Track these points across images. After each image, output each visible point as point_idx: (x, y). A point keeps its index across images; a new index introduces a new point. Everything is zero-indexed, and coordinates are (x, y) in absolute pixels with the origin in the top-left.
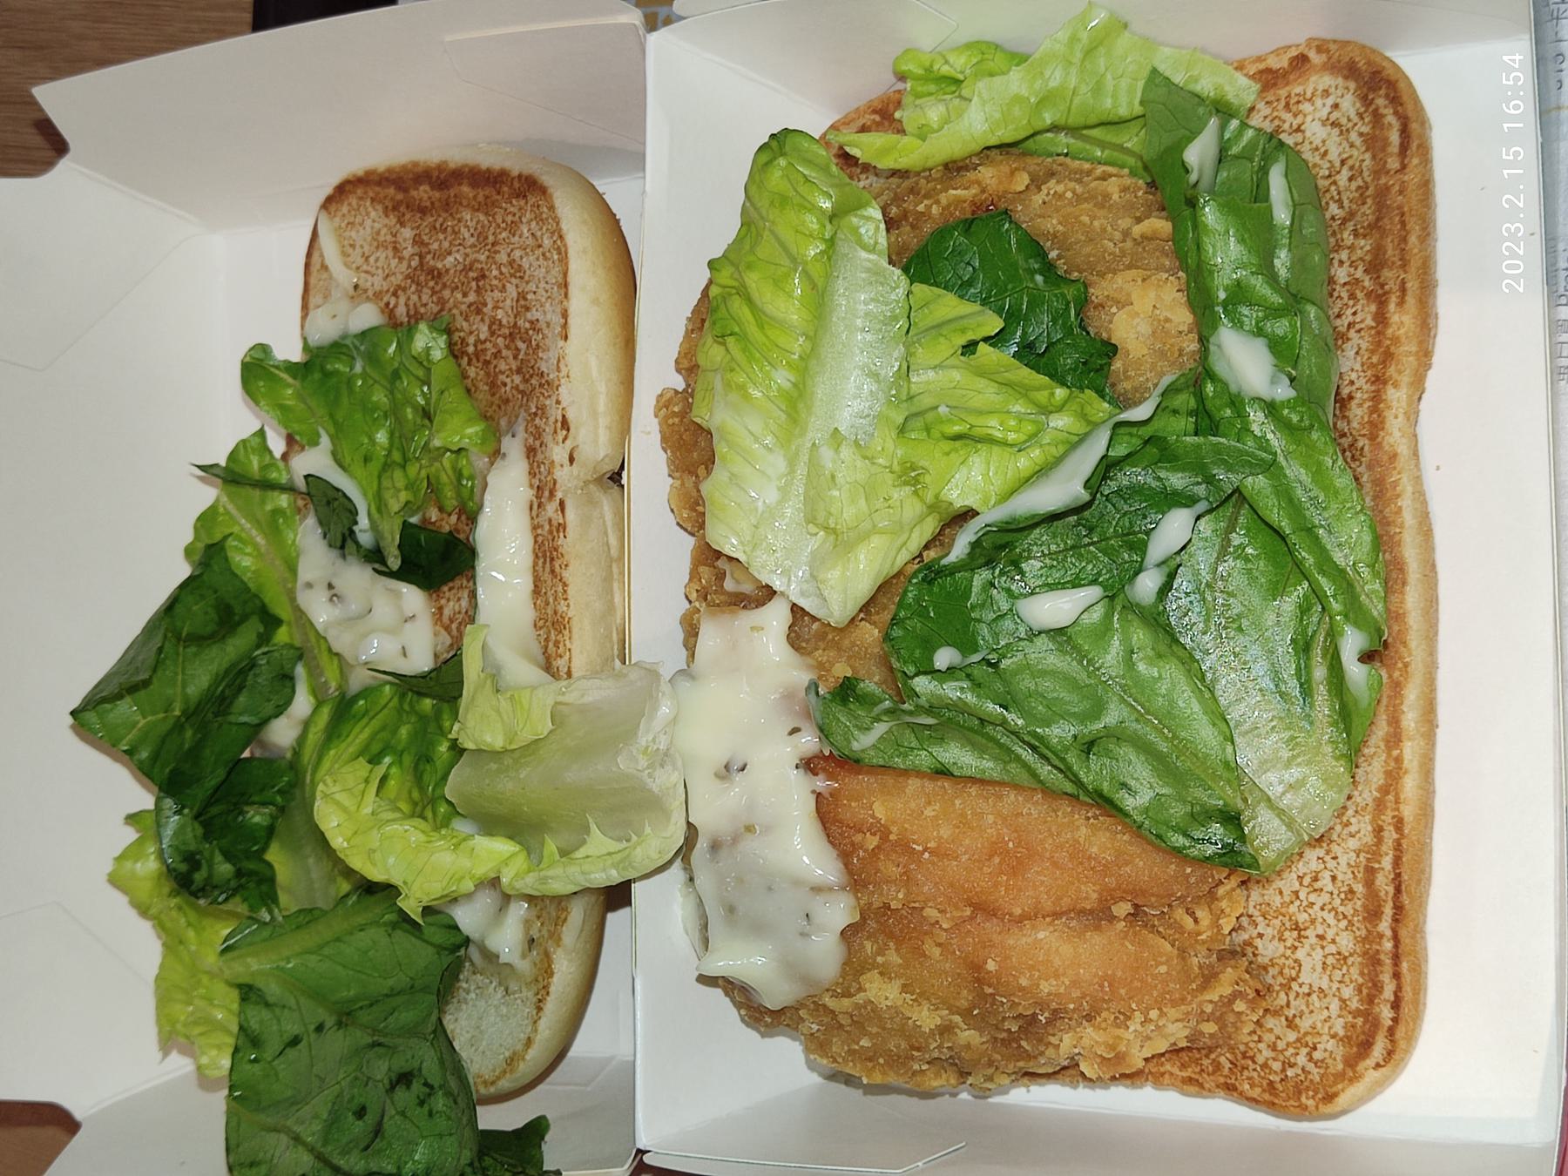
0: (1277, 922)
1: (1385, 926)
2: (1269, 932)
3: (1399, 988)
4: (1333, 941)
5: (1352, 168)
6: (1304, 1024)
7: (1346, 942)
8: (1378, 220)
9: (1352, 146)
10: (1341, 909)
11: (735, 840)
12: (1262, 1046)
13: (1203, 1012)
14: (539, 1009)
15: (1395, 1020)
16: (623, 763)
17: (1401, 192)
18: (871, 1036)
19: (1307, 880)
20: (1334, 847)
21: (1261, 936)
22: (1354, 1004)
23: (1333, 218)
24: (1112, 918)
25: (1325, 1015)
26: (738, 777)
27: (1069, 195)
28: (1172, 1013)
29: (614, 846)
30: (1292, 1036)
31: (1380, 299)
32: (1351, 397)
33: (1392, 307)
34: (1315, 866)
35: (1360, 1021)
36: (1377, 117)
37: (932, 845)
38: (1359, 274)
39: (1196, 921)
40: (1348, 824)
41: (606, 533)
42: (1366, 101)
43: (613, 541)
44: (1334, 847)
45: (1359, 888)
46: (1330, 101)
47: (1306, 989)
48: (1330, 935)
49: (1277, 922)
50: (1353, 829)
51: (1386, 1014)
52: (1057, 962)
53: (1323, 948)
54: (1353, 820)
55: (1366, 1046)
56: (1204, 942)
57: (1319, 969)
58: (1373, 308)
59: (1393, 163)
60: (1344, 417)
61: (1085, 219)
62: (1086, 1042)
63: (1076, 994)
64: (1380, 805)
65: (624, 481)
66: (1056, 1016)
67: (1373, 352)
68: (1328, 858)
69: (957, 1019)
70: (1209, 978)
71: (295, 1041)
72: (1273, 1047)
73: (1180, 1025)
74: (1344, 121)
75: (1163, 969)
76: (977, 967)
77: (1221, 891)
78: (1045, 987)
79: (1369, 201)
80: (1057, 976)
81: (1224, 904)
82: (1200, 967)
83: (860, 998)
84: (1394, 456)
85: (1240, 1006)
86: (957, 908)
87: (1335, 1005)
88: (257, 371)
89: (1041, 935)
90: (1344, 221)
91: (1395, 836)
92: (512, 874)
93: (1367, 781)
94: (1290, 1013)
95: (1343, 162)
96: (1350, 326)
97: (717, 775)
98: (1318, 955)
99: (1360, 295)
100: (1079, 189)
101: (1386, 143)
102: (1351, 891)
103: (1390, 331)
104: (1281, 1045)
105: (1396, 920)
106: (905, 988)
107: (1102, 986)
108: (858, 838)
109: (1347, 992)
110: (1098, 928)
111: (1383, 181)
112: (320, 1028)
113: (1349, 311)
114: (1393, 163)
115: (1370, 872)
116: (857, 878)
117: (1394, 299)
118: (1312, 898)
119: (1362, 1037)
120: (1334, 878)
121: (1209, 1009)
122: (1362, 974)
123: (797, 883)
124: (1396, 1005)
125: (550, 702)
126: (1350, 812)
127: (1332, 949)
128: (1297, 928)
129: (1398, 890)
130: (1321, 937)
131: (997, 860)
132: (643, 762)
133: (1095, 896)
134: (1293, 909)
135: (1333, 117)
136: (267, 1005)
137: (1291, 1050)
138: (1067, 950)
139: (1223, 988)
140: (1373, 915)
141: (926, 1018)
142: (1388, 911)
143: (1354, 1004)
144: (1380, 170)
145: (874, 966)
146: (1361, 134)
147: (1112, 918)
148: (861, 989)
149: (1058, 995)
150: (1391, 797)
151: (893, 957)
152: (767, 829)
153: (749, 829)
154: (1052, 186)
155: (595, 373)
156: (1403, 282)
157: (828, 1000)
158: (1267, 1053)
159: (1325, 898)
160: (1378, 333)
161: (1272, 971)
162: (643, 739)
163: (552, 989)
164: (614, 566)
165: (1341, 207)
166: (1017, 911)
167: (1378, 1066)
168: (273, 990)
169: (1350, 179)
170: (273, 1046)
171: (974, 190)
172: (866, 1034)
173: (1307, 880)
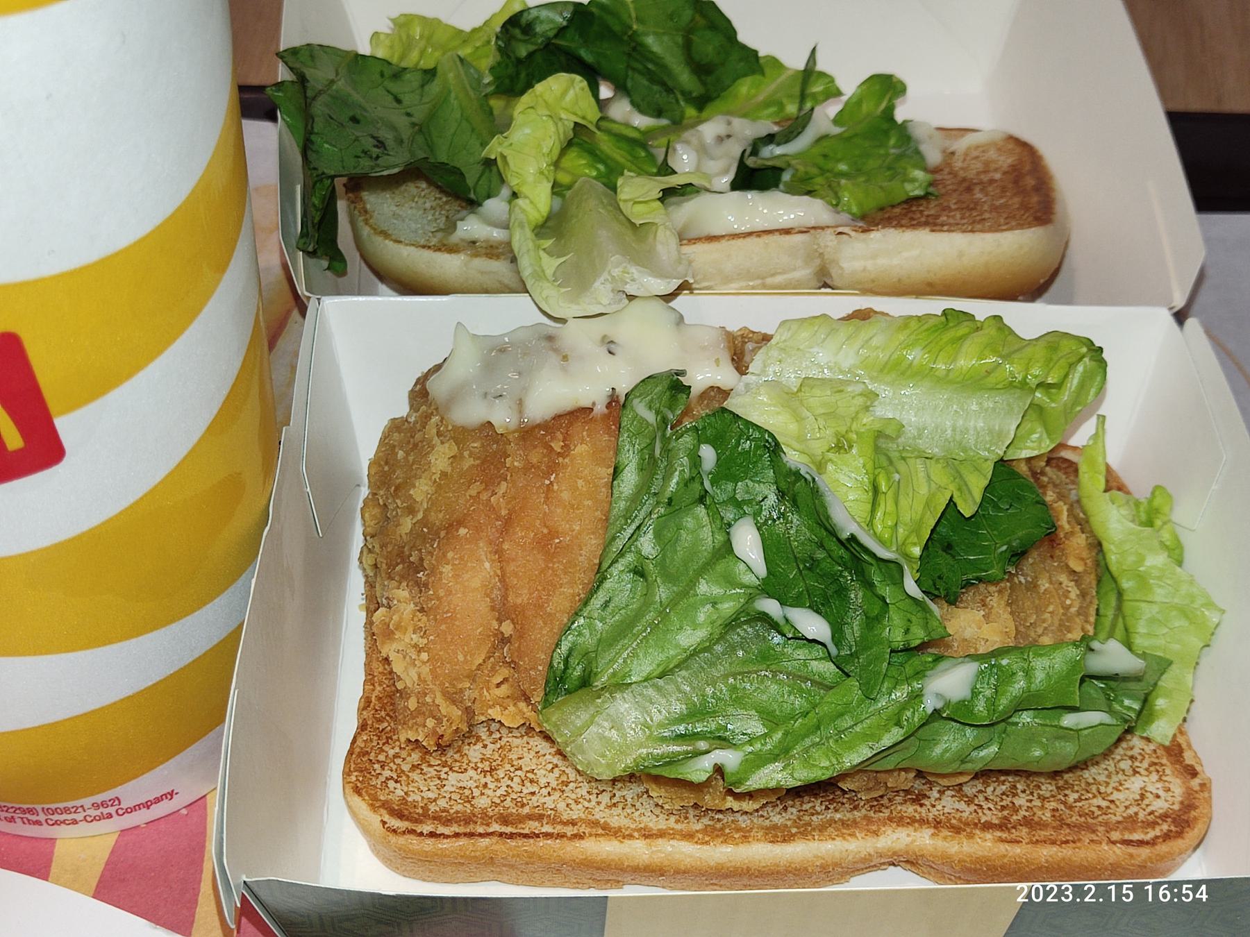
0: (496, 756)
1: (495, 827)
2: (488, 752)
3: (447, 837)
4: (482, 794)
5: (1108, 807)
6: (415, 776)
7: (482, 802)
8: (1068, 825)
9: (1127, 807)
10: (509, 799)
11: (556, 350)
12: (397, 750)
13: (426, 695)
14: (424, 247)
15: (421, 834)
16: (616, 258)
17: (1092, 841)
18: (406, 458)
20: (558, 794)
21: (485, 746)
22: (432, 808)
23: (1066, 795)
24: (500, 621)
25: (421, 789)
26: (604, 350)
27: (1068, 602)
28: (426, 670)
29: (549, 272)
30: (406, 767)
31: (1002, 826)
32: (921, 805)
33: (999, 834)
34: (543, 782)
35: (420, 811)
36: (1153, 824)
37: (556, 487)
38: (1023, 813)
39: (498, 685)
40: (577, 802)
41: (784, 272)
42: (1164, 817)
43: (778, 279)
44: (558, 794)
45: (526, 810)
46: (1161, 793)
47: (443, 776)
49: (496, 756)
50: (573, 806)
51: (426, 828)
52: (466, 576)
54: (580, 806)
55: (400, 815)
56: (481, 695)
57: (461, 784)
58: (996, 821)
59: (1115, 836)
60: (905, 801)
61: (1051, 608)
62: (402, 606)
63: (441, 593)
64: (596, 824)
65: (823, 290)
66: (422, 586)
67: (960, 820)
68: (549, 789)
69: (420, 516)
70: (453, 698)
71: (398, 101)
72: (396, 756)
73: (416, 678)
74: (1146, 802)
75: (461, 658)
76: (460, 523)
77: (522, 705)
78: (447, 569)
79: (1083, 819)
80: (456, 576)
81: (511, 708)
82: (462, 691)
83: (436, 440)
84: (876, 833)
85: (430, 723)
86: (507, 503)
87: (431, 795)
88: (887, 87)
89: (487, 565)
90: (1065, 803)
91: (569, 834)
92: (524, 206)
93: (611, 815)
94: (423, 766)
95: (1112, 801)
96: (980, 806)
97: (604, 337)
98: (472, 784)
99: (1005, 813)
100: (1073, 610)
101: (1133, 830)
102: (523, 805)
103: (977, 832)
104: (398, 761)
105: (501, 835)
106: (444, 474)
107: (447, 612)
108: (560, 436)
109: (442, 803)
110: (493, 609)
111: (1101, 829)
112: (408, 115)
113: (992, 807)
114: (1115, 836)
115: (540, 818)
116: (528, 433)
117: (1004, 835)
118: (517, 780)
119: (406, 813)
120: (533, 794)
121: (428, 699)
122: (457, 812)
123: (525, 389)
124: (432, 835)
125: (656, 221)
126: (586, 804)
127: (476, 793)
128: (492, 770)
129: (526, 836)
130: (485, 785)
131: (545, 531)
132: (616, 272)
133: (519, 601)
134: (508, 767)
135: (1148, 795)
136: (422, 86)
137: (394, 767)
138: (476, 583)
139: (445, 708)
140: (505, 820)
141: (421, 491)
142: (509, 830)
143: (432, 808)
144: (1109, 827)
145: (461, 450)
146: (1136, 814)
147: (500, 621)
148: (442, 443)
149: (440, 579)
150: (600, 831)
151: (468, 462)
152: (564, 370)
153: (565, 358)
154: (1074, 592)
155: (905, 254)
156: (1019, 842)
157: (435, 419)
158: (391, 752)
159: (517, 788)
160: (976, 825)
161: (457, 756)
162: (634, 270)
163: (438, 254)
164: (759, 282)
165: (1075, 801)
166: (506, 546)
167: (384, 823)
168: (435, 88)
169: (1099, 807)
170: (394, 87)
171: (1067, 527)
172: (408, 454)
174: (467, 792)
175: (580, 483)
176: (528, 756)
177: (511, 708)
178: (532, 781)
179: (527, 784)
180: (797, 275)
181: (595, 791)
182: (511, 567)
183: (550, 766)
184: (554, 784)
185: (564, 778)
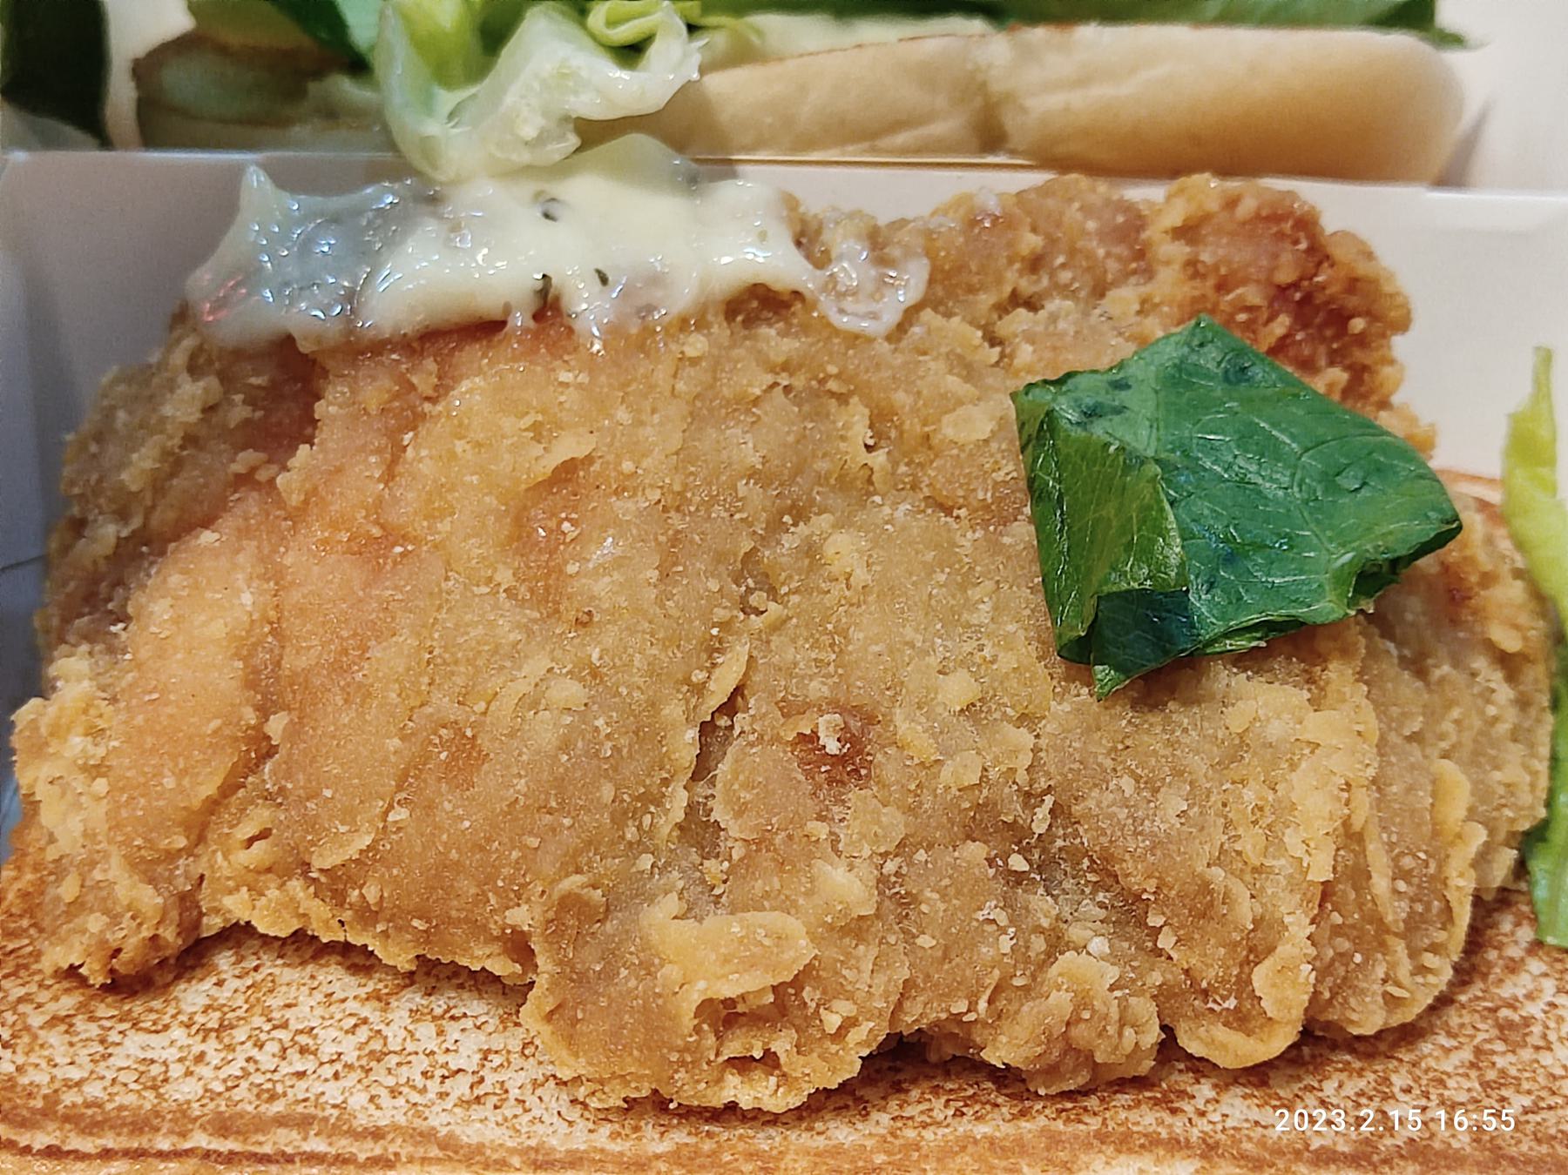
2: (223, 995)
4: (189, 1073)
19: (303, 1040)
20: (359, 1074)
21: (219, 984)
34: (328, 1051)
39: (250, 842)
44: (356, 1075)
47: (114, 1037)
48: (201, 1070)
53: (181, 1060)
57: (149, 1055)
61: (1456, 713)
68: (338, 1066)
75: (169, 782)
81: (273, 893)
98: (172, 1054)
118: (273, 1047)
120: (301, 1075)
127: (176, 1071)
128: (222, 1028)
130: (200, 1058)
134: (258, 1021)
138: (218, 629)
151: (239, 412)
173: (303, 1040)
174: (156, 1070)
175: (459, 446)
176: (306, 1002)
177: (273, 893)
178: (304, 1051)
179: (293, 1054)
180: (938, 129)
181: (439, 1072)
182: (296, 596)
183: (353, 1021)
184: (351, 1057)
185: (376, 1045)
